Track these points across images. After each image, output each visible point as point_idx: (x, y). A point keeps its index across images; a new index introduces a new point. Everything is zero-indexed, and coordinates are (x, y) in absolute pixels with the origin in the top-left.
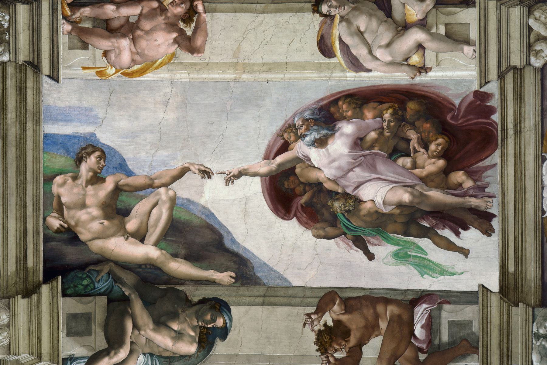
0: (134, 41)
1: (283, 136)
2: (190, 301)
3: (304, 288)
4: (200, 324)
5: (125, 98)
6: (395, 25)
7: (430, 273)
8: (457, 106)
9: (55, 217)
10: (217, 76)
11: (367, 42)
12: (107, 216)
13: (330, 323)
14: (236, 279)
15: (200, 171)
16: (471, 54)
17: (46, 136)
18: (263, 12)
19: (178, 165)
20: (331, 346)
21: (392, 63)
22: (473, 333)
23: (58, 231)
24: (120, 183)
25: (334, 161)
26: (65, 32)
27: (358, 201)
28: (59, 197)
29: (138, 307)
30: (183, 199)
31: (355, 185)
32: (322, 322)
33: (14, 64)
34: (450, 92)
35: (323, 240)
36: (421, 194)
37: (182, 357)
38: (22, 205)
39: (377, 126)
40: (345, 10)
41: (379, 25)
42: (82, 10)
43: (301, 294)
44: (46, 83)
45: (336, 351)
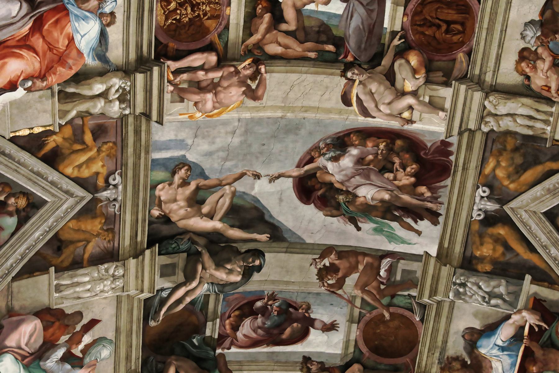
0: (216, 94)
1: (311, 153)
2: (240, 252)
3: (313, 244)
4: (245, 264)
5: (207, 131)
6: (396, 92)
7: (395, 241)
8: (429, 147)
9: (156, 210)
10: (270, 114)
11: (376, 100)
12: (190, 206)
13: (328, 264)
14: (270, 238)
15: (253, 174)
16: (444, 117)
17: (153, 161)
18: (306, 73)
19: (239, 171)
20: (326, 277)
21: (391, 115)
22: (417, 277)
23: (158, 217)
24: (199, 185)
25: (342, 170)
26: (169, 92)
27: (356, 196)
28: (159, 197)
29: (206, 257)
30: (240, 192)
31: (355, 187)
32: (322, 264)
33: (133, 115)
34: (425, 138)
35: (329, 217)
36: (397, 196)
37: (231, 283)
38: (135, 205)
39: (374, 152)
40: (363, 77)
41: (385, 90)
42: (182, 76)
43: (311, 247)
44: (154, 126)
45: (329, 279)
